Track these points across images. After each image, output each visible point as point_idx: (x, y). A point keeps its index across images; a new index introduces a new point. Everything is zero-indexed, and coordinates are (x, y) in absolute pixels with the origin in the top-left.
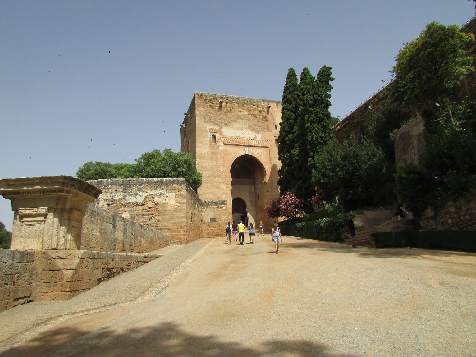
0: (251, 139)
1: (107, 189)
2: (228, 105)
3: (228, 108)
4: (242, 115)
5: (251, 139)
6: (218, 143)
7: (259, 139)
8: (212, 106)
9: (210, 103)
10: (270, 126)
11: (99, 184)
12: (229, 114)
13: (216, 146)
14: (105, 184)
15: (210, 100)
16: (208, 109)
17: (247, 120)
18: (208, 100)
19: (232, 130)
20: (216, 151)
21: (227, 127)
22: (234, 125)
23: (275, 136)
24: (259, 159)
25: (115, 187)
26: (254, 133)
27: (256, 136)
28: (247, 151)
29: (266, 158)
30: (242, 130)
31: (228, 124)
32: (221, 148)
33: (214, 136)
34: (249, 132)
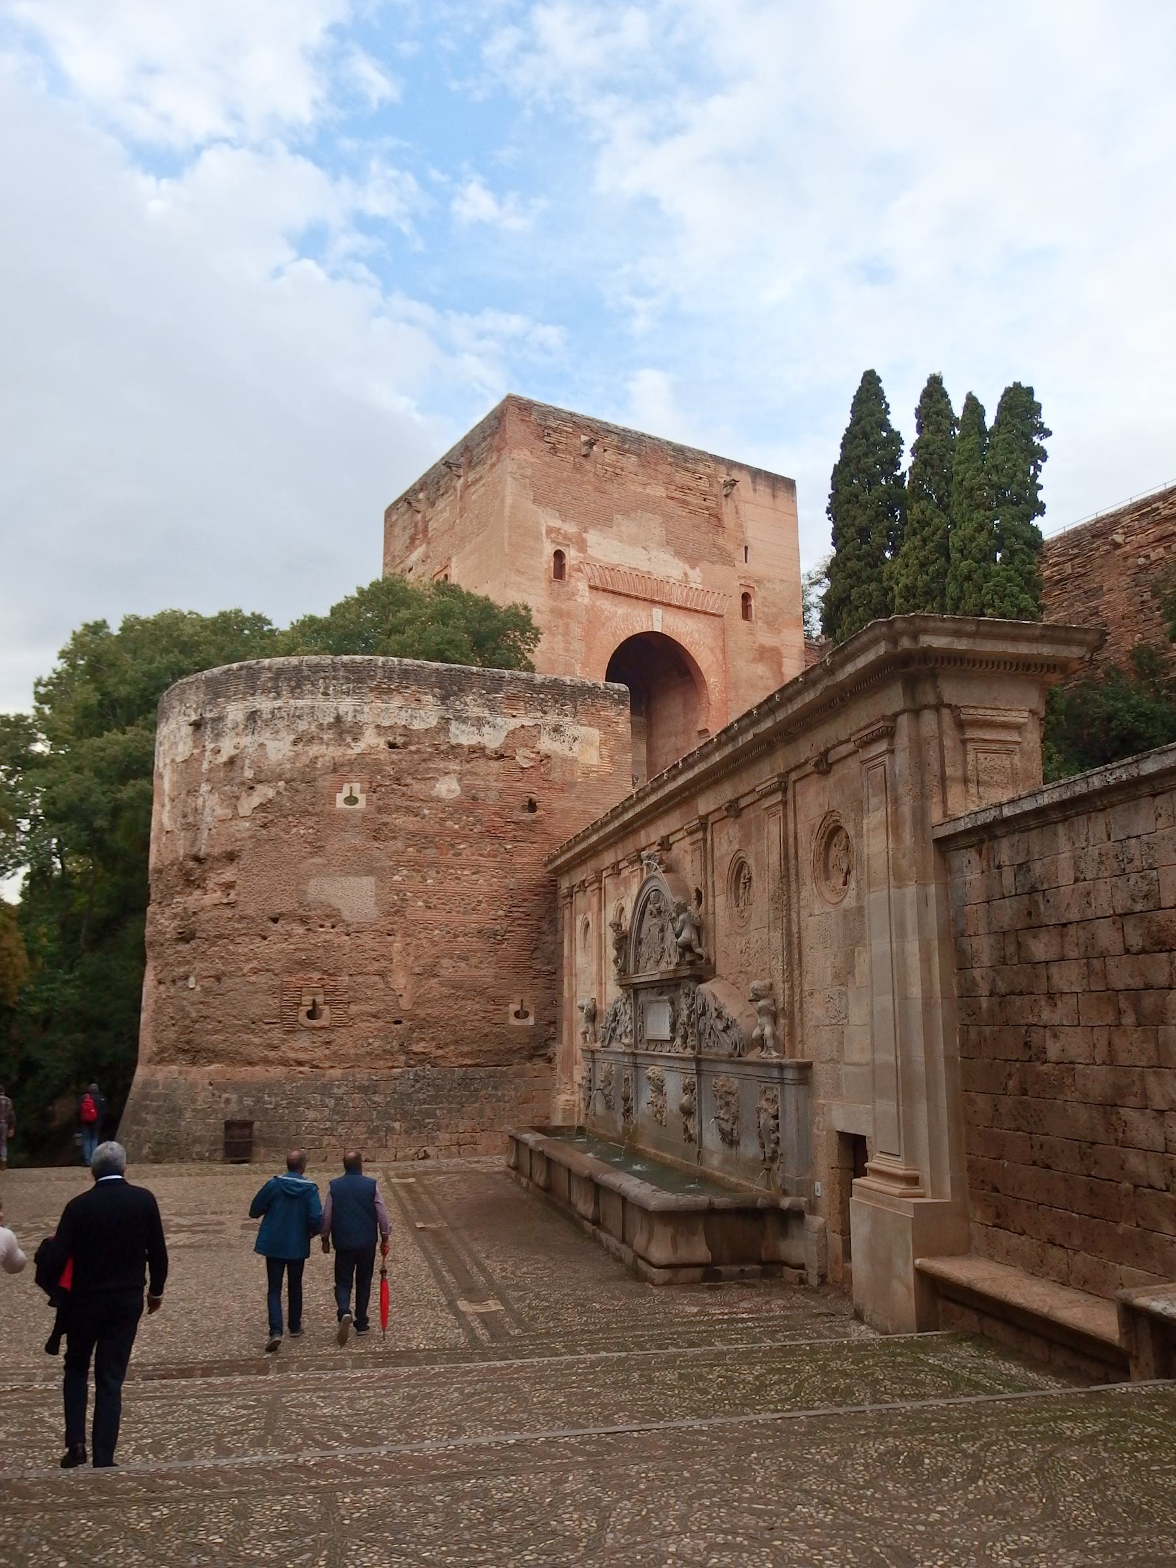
0: (672, 581)
1: (389, 691)
2: (609, 457)
3: (609, 465)
4: (648, 496)
5: (672, 581)
6: (573, 580)
7: (694, 586)
8: (560, 450)
9: (552, 440)
10: (730, 547)
11: (360, 672)
12: (608, 487)
13: (565, 589)
14: (380, 673)
15: (555, 430)
16: (547, 459)
17: (662, 515)
18: (548, 427)
19: (616, 542)
20: (565, 606)
21: (600, 530)
22: (623, 529)
23: (742, 582)
24: (692, 651)
25: (413, 688)
26: (681, 564)
27: (686, 574)
28: (657, 621)
29: (712, 650)
30: (645, 548)
31: (604, 520)
32: (579, 599)
33: (559, 555)
34: (667, 557)
